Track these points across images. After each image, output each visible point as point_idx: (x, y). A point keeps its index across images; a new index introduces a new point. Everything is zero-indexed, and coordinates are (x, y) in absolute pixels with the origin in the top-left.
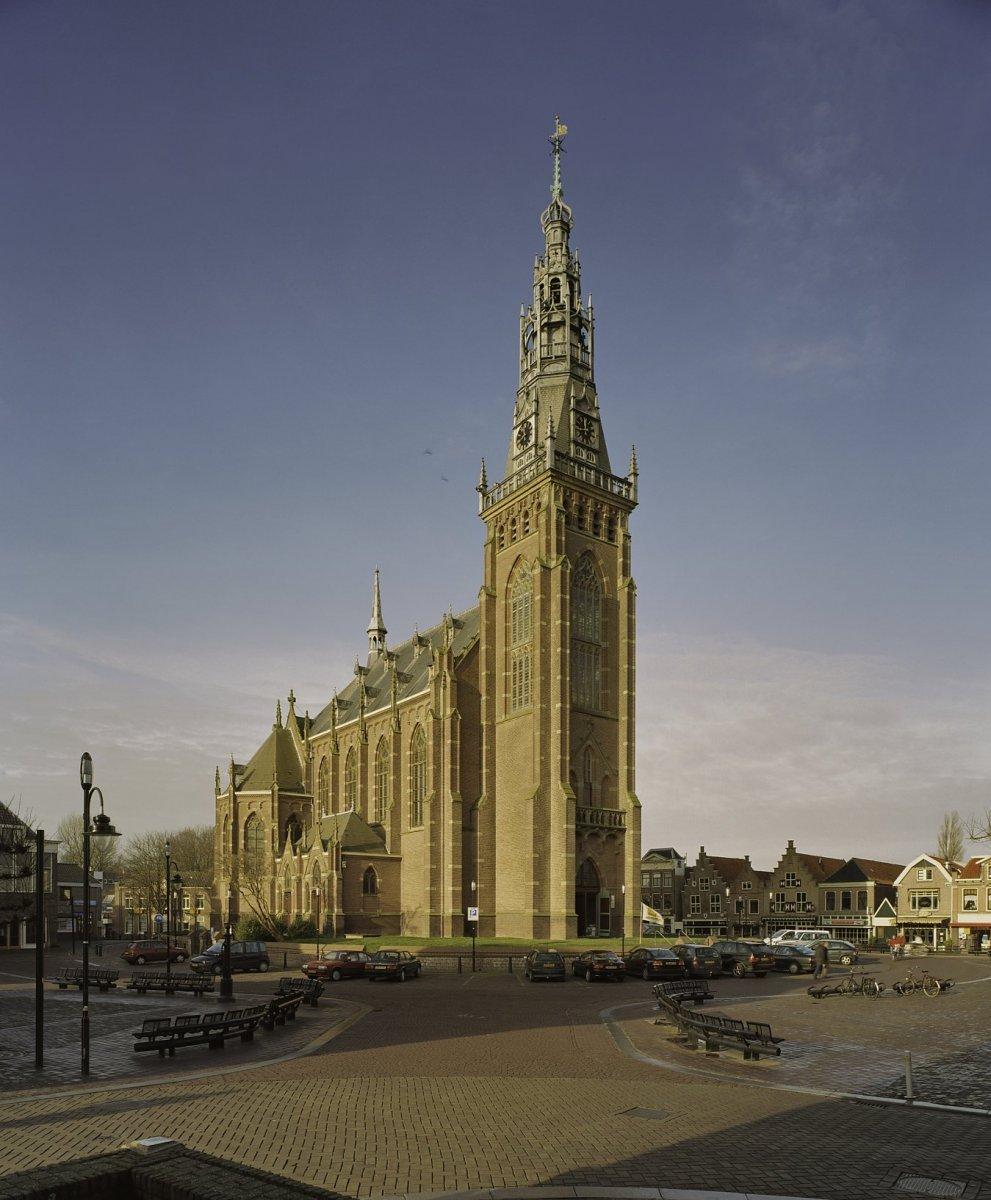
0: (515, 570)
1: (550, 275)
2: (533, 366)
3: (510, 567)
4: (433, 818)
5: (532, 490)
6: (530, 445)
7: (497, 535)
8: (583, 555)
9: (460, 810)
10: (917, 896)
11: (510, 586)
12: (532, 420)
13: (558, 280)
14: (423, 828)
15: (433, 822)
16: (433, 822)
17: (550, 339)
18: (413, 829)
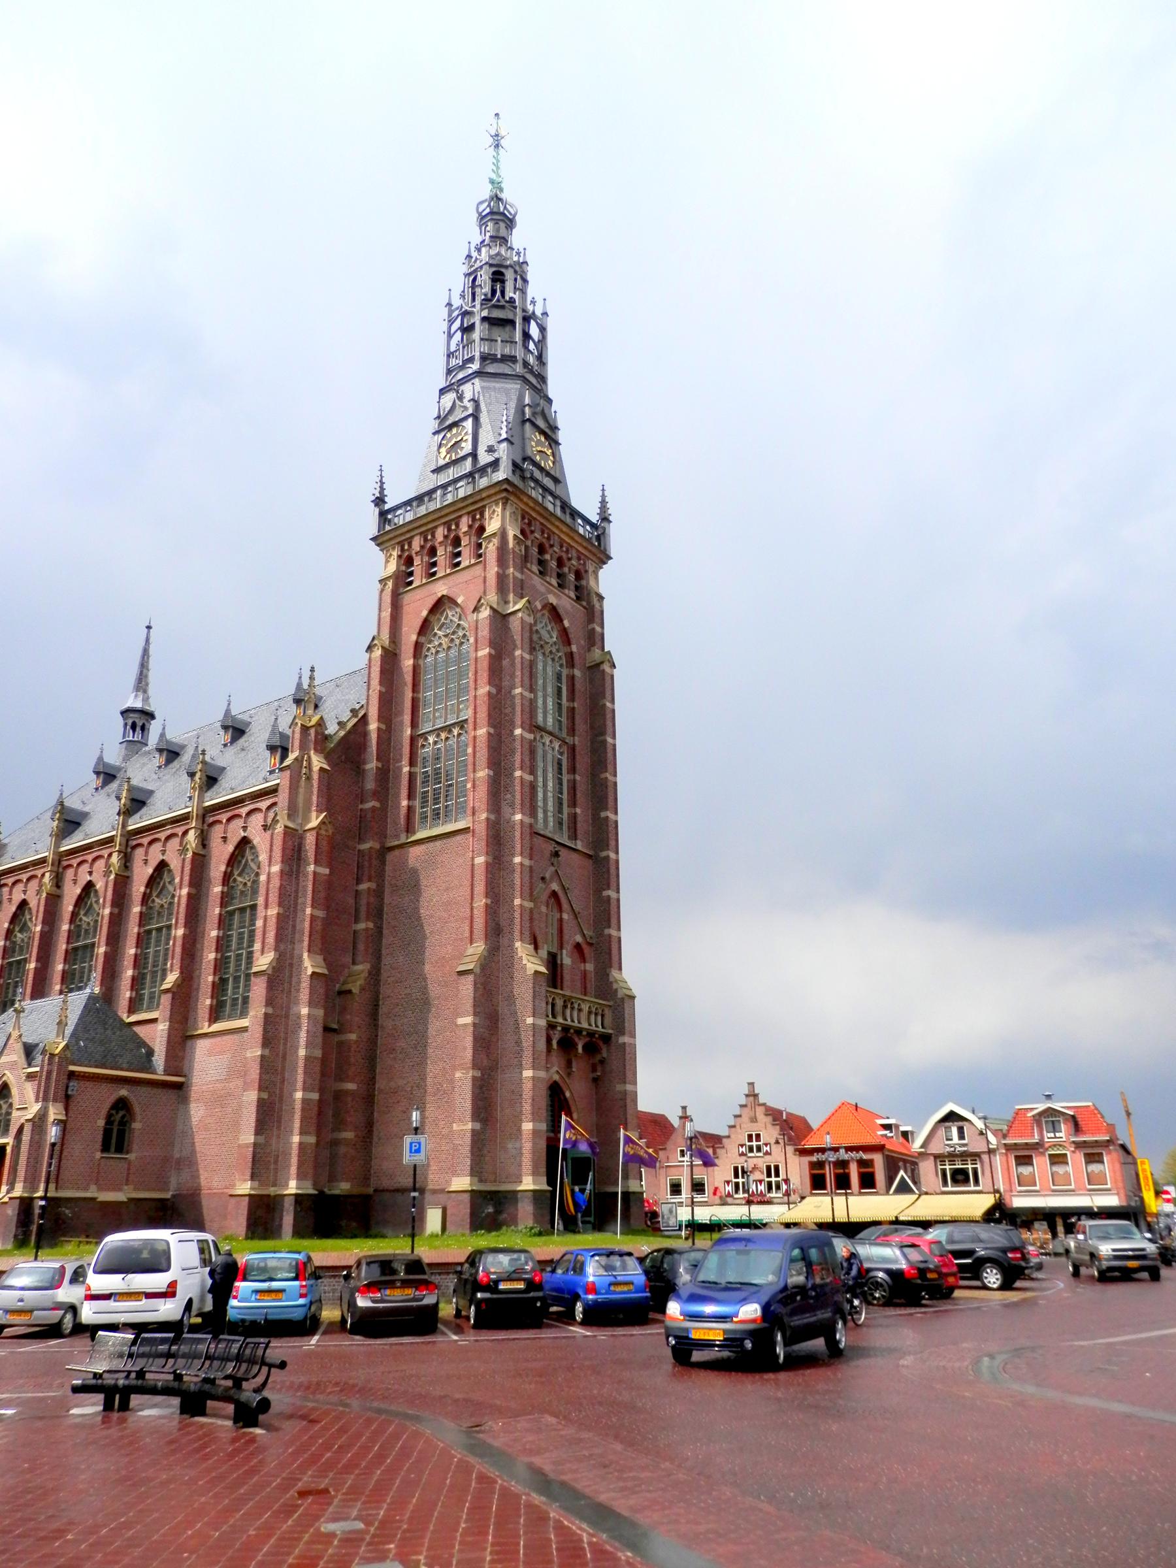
0: (432, 619)
1: (491, 265)
2: (471, 360)
3: (425, 613)
4: (269, 1002)
6: (461, 454)
7: (403, 568)
9: (322, 991)
10: (948, 1167)
11: (422, 639)
14: (244, 1023)
15: (270, 1011)
16: (270, 1011)
18: (216, 1027)
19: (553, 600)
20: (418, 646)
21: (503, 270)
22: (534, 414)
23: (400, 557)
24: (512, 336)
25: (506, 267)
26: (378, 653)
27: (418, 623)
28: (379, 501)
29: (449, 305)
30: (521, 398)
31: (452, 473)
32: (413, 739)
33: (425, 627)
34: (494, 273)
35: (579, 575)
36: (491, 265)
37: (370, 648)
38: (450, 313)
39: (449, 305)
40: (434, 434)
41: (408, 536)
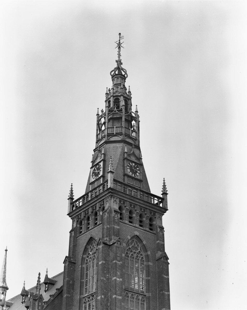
0: (89, 247)
1: (114, 97)
5: (100, 200)
6: (100, 176)
8: (132, 238)
11: (85, 256)
12: (101, 164)
13: (119, 99)
17: (113, 125)
19: (137, 233)
20: (83, 259)
21: (119, 98)
22: (129, 155)
23: (77, 221)
24: (121, 124)
25: (120, 96)
26: (67, 263)
27: (82, 249)
28: (71, 198)
29: (98, 115)
30: (123, 149)
31: (96, 185)
32: (80, 300)
33: (86, 250)
34: (115, 99)
35: (151, 220)
36: (114, 97)
37: (64, 262)
38: (98, 117)
39: (98, 115)
40: (91, 168)
41: (80, 212)
